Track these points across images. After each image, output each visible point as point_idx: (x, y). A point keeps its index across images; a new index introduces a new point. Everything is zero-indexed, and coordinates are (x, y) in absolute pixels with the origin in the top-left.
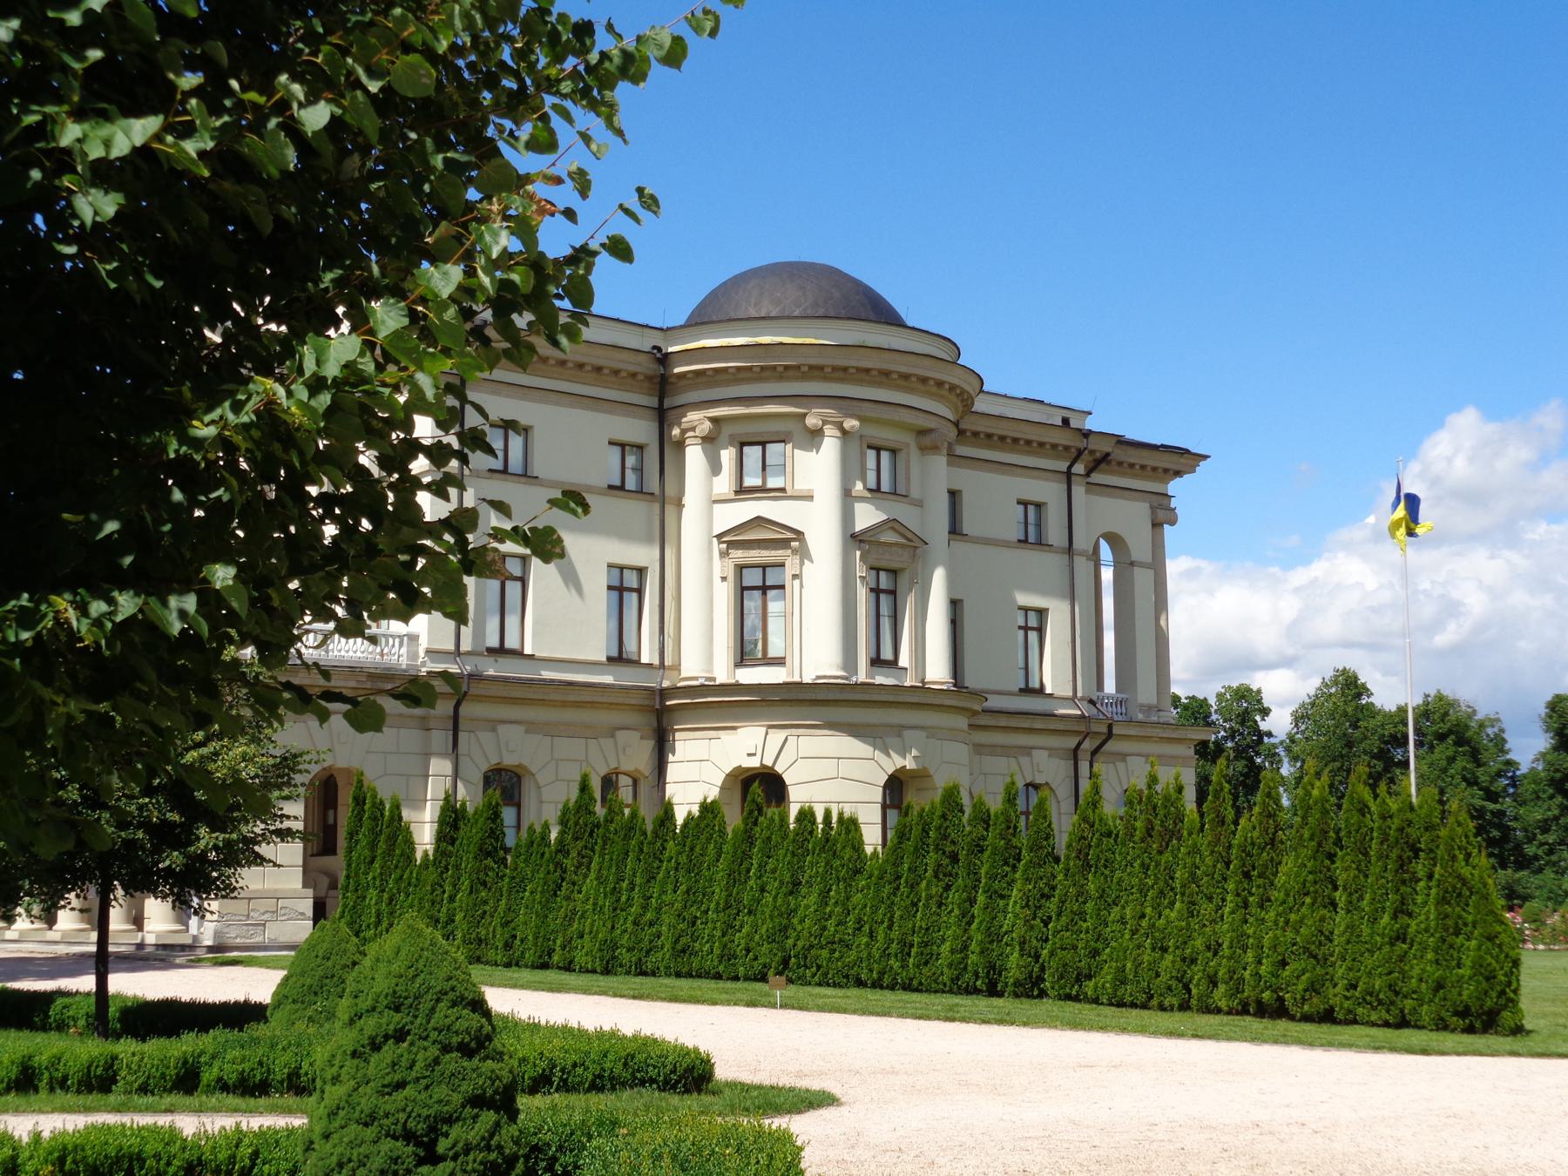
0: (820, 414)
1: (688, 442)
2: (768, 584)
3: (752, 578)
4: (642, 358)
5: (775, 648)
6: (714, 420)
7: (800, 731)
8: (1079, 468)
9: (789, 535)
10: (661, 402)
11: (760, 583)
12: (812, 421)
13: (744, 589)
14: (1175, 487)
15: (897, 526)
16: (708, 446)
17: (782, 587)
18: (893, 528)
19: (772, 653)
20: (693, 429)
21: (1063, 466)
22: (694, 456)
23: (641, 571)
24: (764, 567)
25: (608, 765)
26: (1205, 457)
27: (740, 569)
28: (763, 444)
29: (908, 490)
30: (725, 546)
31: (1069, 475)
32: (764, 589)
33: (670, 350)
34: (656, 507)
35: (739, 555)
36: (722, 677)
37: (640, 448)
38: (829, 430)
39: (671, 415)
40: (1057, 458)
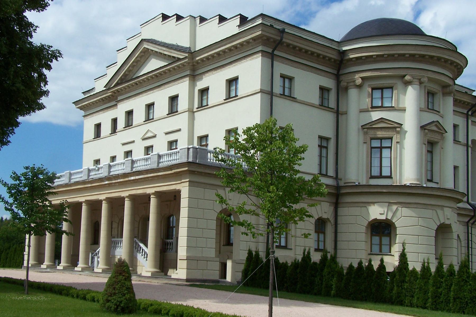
1: (349, 88)
2: (383, 146)
3: (376, 144)
5: (386, 172)
6: (363, 78)
11: (380, 146)
13: (372, 148)
15: (438, 124)
17: (390, 148)
18: (436, 125)
19: (384, 174)
22: (353, 93)
23: (327, 139)
24: (381, 139)
25: (319, 216)
28: (382, 89)
29: (439, 109)
30: (366, 130)
32: (381, 148)
33: (345, 48)
34: (335, 115)
35: (371, 133)
36: (364, 183)
37: (328, 90)
39: (342, 78)
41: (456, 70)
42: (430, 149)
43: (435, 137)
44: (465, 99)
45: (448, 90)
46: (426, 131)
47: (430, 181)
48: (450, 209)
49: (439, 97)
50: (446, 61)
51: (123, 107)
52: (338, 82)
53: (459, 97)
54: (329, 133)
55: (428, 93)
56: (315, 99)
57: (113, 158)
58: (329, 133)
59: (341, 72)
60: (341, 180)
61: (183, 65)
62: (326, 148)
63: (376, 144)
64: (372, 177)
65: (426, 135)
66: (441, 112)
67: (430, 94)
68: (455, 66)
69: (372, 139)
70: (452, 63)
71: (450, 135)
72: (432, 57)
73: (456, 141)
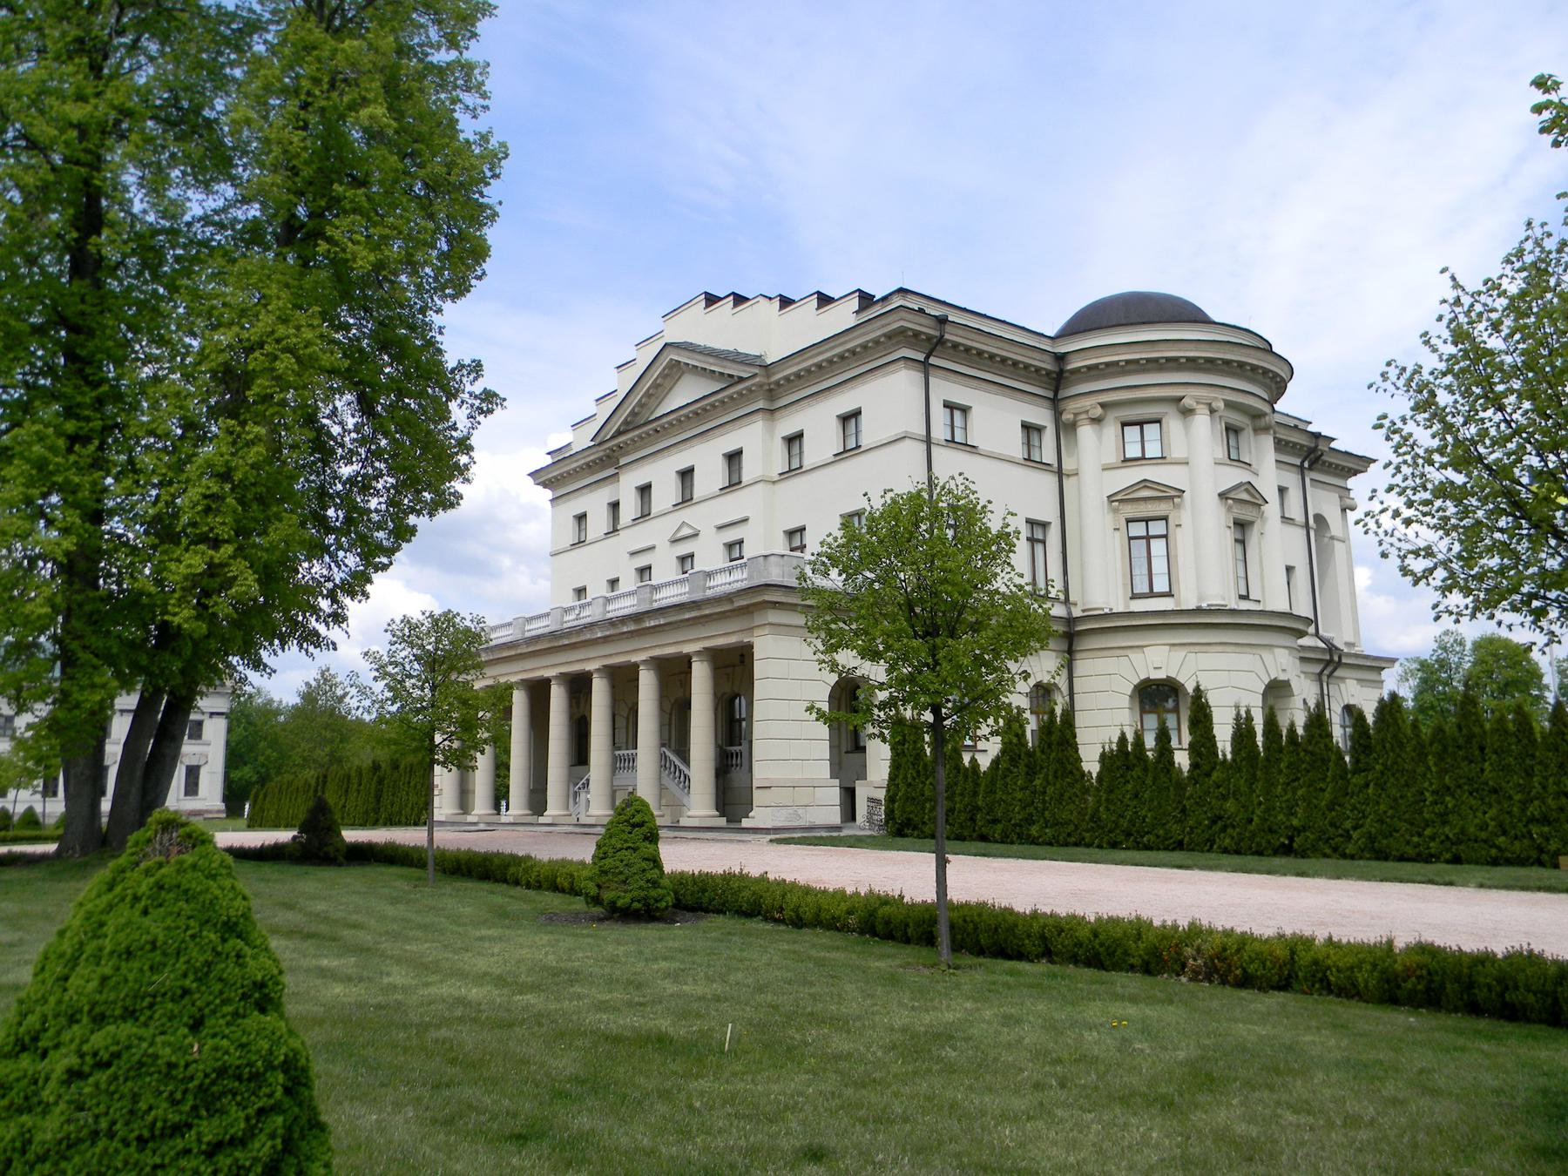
0: (1194, 397)
4: (1047, 358)
5: (1161, 585)
7: (1197, 648)
8: (1306, 465)
9: (1173, 493)
10: (1056, 393)
12: (1187, 402)
13: (1131, 538)
14: (1351, 483)
16: (1096, 426)
18: (1247, 490)
20: (1087, 412)
21: (1298, 462)
23: (1044, 525)
24: (1147, 520)
26: (1375, 461)
27: (1128, 521)
28: (1141, 424)
31: (1301, 468)
32: (1148, 538)
34: (1055, 479)
35: (1130, 510)
37: (1039, 430)
38: (1202, 411)
39: (1062, 405)
40: (1298, 456)
41: (1273, 386)
42: (1240, 537)
43: (1245, 514)
44: (1296, 438)
45: (1263, 422)
46: (1230, 502)
47: (1245, 597)
48: (1286, 652)
49: (1248, 435)
50: (1254, 368)
51: (629, 483)
52: (1057, 414)
53: (1284, 435)
54: (1049, 514)
55: (1227, 429)
56: (1014, 445)
57: (614, 583)
58: (1049, 514)
59: (1062, 394)
60: (1075, 604)
61: (749, 390)
62: (1044, 542)
63: (1138, 529)
64: (1134, 597)
65: (1229, 509)
66: (1253, 463)
67: (1232, 430)
68: (1271, 378)
69: (1128, 521)
70: (1266, 372)
71: (1272, 509)
72: (1227, 362)
73: (1286, 520)
